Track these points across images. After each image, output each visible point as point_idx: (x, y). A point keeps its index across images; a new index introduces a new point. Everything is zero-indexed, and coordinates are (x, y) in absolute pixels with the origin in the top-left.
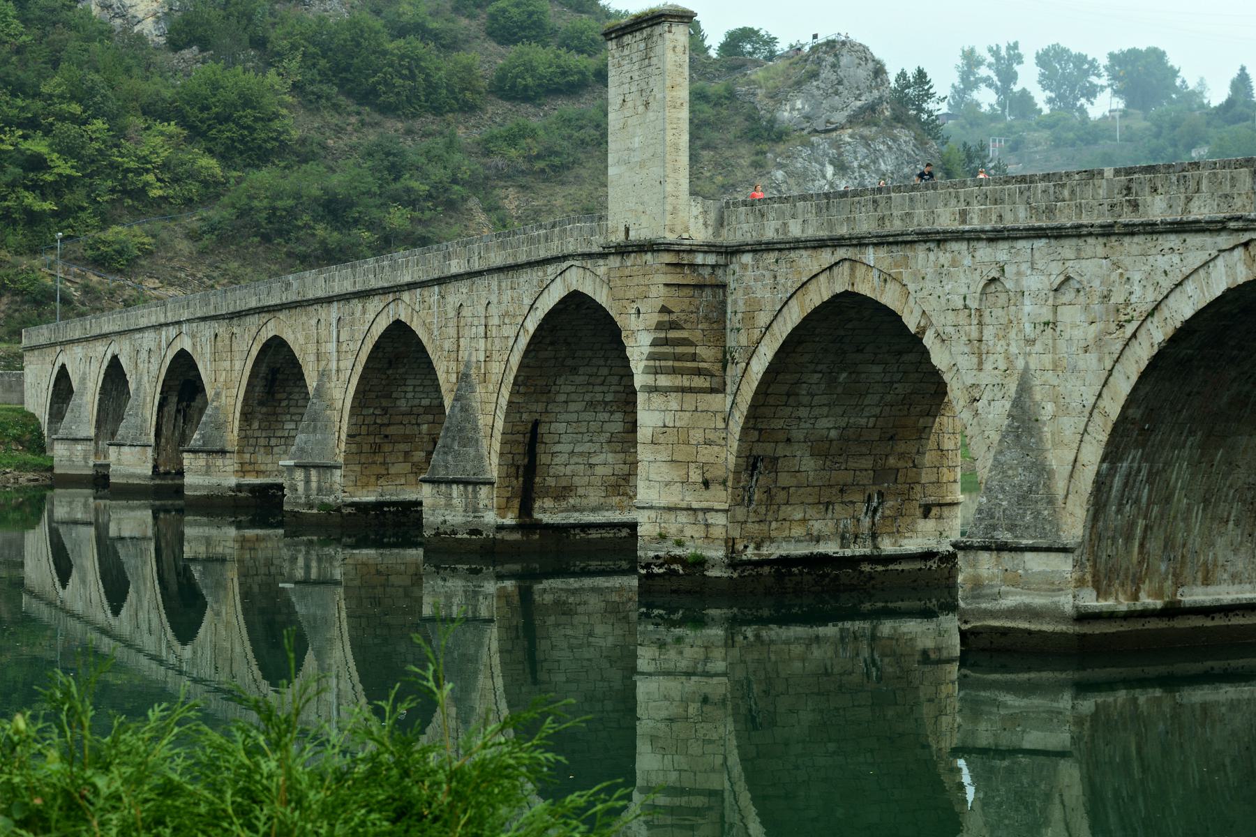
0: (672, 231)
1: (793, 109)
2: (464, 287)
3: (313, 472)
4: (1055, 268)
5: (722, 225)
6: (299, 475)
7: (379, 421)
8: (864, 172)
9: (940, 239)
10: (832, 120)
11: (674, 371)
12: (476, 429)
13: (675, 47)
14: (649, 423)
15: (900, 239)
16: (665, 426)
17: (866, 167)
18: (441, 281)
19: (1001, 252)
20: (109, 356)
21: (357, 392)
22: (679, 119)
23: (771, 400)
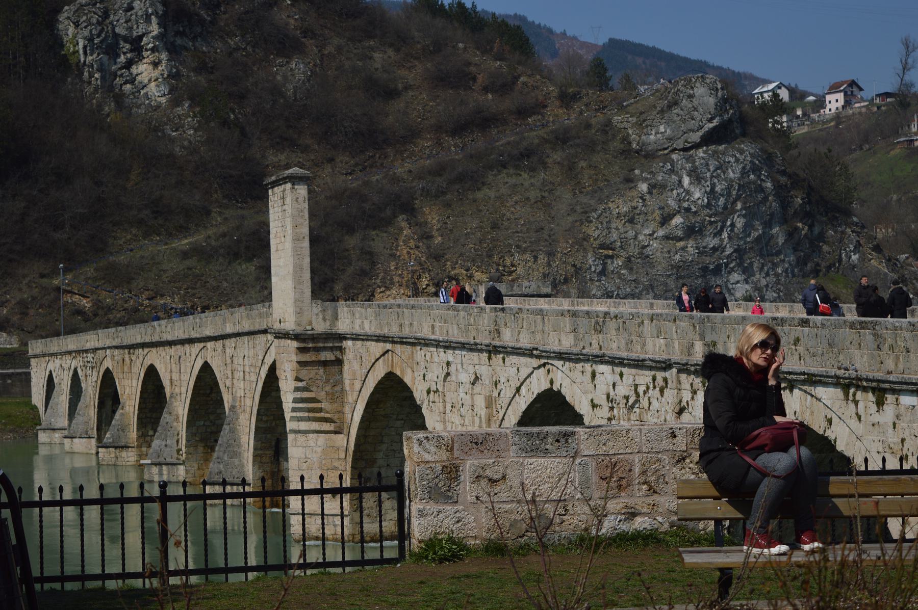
1: (657, 133)
3: (164, 467)
4: (471, 369)
6: (155, 470)
8: (716, 181)
10: (689, 140)
11: (309, 419)
12: (239, 446)
13: (297, 198)
14: (296, 456)
15: (404, 340)
16: (306, 458)
19: (450, 355)
20: (73, 368)
22: (302, 248)
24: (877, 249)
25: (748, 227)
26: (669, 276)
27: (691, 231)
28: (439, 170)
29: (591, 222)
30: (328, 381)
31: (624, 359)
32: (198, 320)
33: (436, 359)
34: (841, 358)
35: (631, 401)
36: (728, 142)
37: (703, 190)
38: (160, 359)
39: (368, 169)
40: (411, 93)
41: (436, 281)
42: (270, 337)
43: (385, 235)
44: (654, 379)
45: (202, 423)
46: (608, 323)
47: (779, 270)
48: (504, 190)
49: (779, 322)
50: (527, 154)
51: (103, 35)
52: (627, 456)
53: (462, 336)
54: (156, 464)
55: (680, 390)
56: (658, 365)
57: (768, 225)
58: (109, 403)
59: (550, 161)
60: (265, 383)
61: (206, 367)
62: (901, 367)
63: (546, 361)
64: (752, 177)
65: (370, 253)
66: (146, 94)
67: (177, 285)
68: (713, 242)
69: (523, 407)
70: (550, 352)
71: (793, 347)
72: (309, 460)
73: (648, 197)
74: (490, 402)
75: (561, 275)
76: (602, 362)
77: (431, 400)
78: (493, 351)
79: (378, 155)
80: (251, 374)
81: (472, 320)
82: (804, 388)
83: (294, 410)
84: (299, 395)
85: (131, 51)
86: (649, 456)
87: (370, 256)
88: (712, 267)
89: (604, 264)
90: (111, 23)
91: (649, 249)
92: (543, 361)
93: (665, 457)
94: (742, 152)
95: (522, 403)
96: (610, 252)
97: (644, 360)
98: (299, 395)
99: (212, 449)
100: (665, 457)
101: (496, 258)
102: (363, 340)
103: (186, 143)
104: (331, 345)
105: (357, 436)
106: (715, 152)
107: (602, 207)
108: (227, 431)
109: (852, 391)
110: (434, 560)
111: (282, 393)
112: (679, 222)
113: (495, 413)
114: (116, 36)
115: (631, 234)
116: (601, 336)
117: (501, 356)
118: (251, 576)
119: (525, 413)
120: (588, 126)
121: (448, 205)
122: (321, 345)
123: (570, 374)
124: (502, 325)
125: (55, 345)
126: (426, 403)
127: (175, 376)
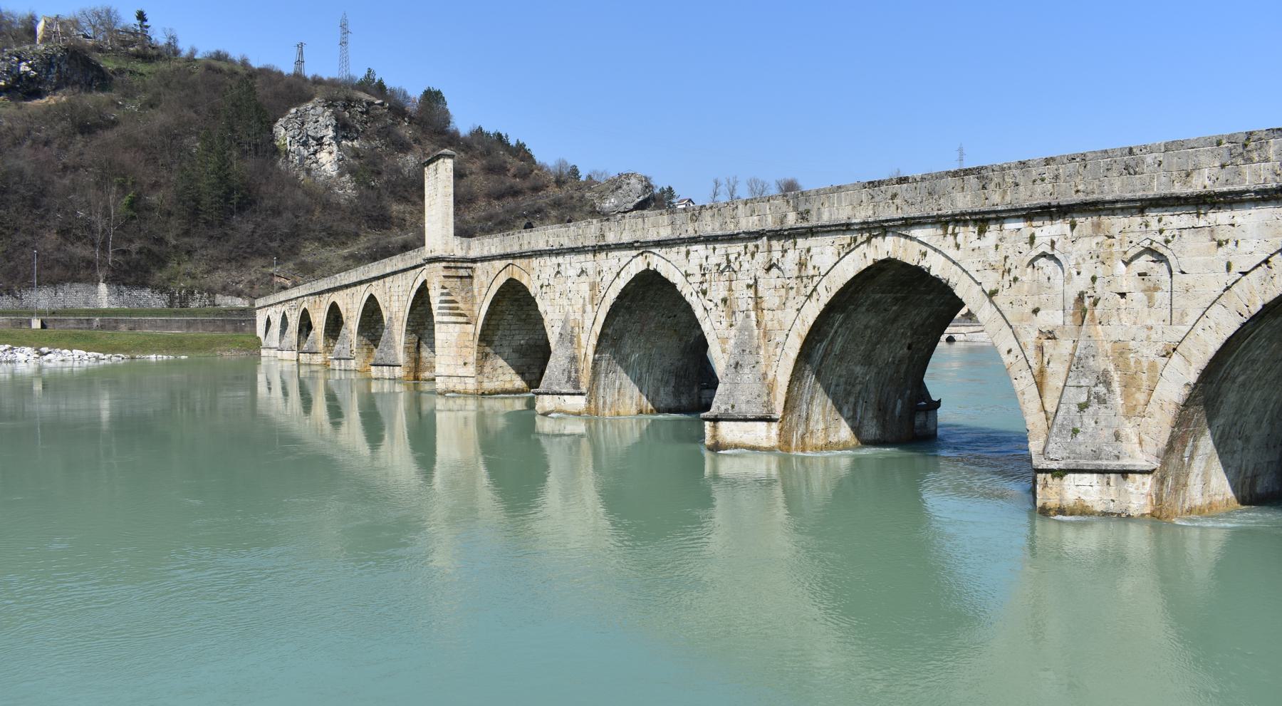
0: (445, 252)
1: (610, 203)
2: (390, 278)
4: (578, 266)
5: (470, 249)
6: (336, 362)
11: (450, 314)
12: (394, 342)
18: (384, 276)
19: (560, 259)
20: (282, 311)
21: (359, 326)
23: (491, 327)
28: (489, 218)
30: (463, 290)
31: (719, 236)
32: (366, 268)
33: (549, 263)
34: (942, 201)
38: (340, 298)
40: (473, 176)
44: (746, 247)
49: (876, 184)
50: (539, 211)
51: (301, 135)
53: (572, 244)
54: (337, 359)
55: (770, 252)
58: (305, 329)
60: (413, 300)
61: (372, 298)
62: (1008, 199)
66: (325, 169)
69: (623, 285)
70: (649, 242)
71: (891, 201)
74: (593, 286)
76: (696, 242)
77: (544, 292)
84: (444, 298)
85: (317, 145)
90: (306, 129)
92: (641, 251)
95: (621, 283)
97: (738, 234)
98: (444, 298)
102: (489, 260)
103: (347, 197)
105: (483, 325)
109: (950, 228)
113: (598, 293)
114: (308, 135)
116: (696, 224)
120: (572, 198)
125: (271, 299)
127: (349, 306)
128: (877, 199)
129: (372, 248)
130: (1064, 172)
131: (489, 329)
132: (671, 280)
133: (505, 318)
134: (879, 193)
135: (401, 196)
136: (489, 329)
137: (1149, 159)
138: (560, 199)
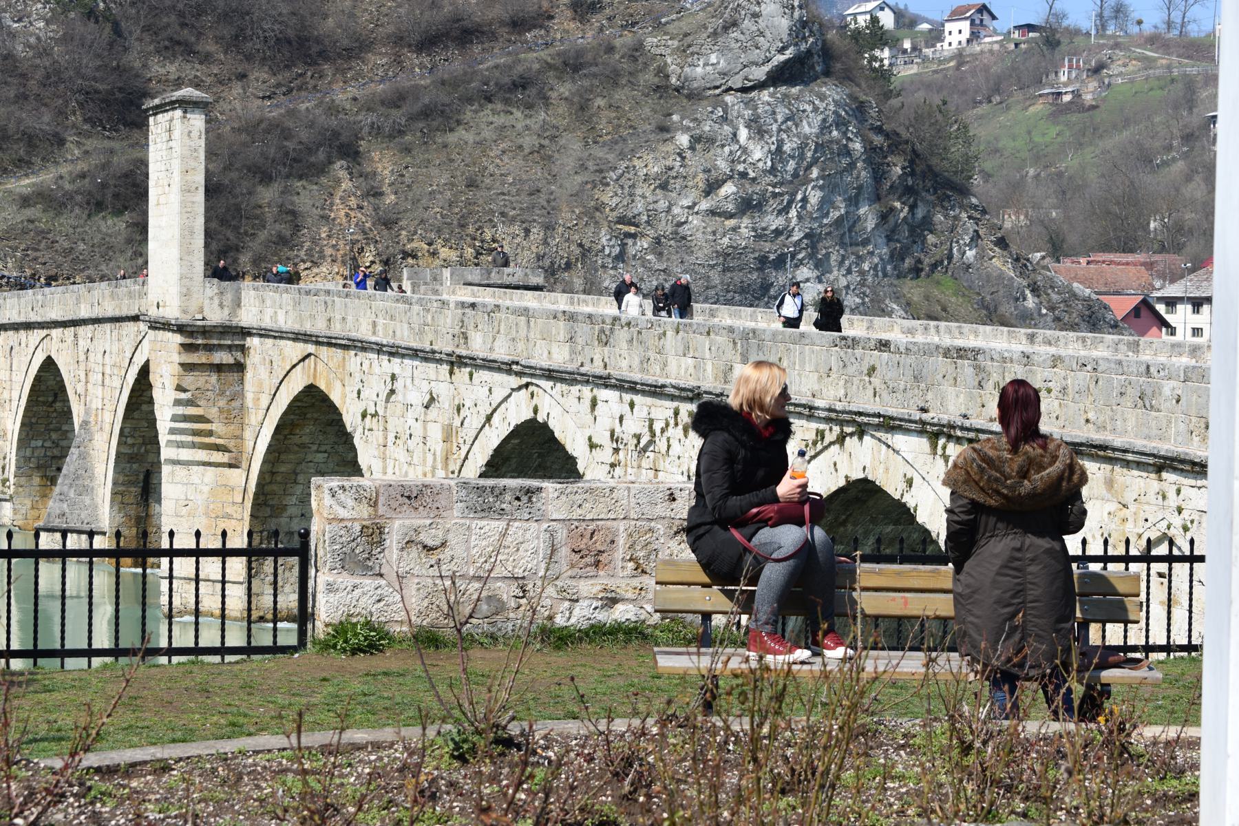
1: (706, 64)
4: (425, 387)
5: (239, 306)
7: (48, 454)
8: (784, 136)
9: (363, 346)
10: (751, 77)
11: (194, 445)
12: (92, 478)
17: (788, 130)
19: (396, 365)
21: (23, 424)
22: (193, 203)
23: (279, 478)
24: (1002, 243)
25: (826, 204)
26: (713, 267)
27: (747, 206)
28: (397, 100)
29: (608, 184)
30: (222, 393)
32: (40, 297)
33: (376, 369)
34: (930, 396)
35: (643, 442)
36: (806, 84)
37: (766, 148)
39: (295, 92)
41: (384, 257)
42: (143, 326)
43: (315, 187)
44: (676, 413)
45: (40, 443)
46: (617, 332)
47: (866, 266)
48: (487, 133)
49: (850, 342)
50: (522, 84)
52: (609, 523)
56: (684, 394)
57: (853, 202)
59: (554, 95)
60: (133, 391)
61: (49, 364)
63: (529, 380)
64: (835, 133)
65: (293, 213)
67: (11, 243)
68: (776, 222)
69: (496, 443)
70: (535, 369)
71: (867, 378)
72: (190, 503)
73: (688, 154)
74: (448, 434)
75: (562, 258)
76: (606, 386)
78: (456, 362)
79: (309, 74)
80: (114, 378)
81: (429, 317)
82: (878, 434)
83: (172, 431)
84: (180, 410)
86: (639, 523)
87: (293, 216)
88: (772, 257)
89: (623, 245)
91: (686, 227)
92: (525, 380)
93: (660, 527)
94: (822, 98)
96: (632, 229)
97: (663, 386)
98: (180, 410)
99: (53, 481)
100: (660, 527)
101: (471, 229)
102: (275, 337)
103: (32, 40)
104: (229, 342)
105: (262, 474)
106: (785, 96)
107: (624, 165)
108: (75, 457)
109: (942, 441)
110: (344, 651)
111: (156, 406)
112: (730, 192)
115: (663, 205)
116: (606, 349)
117: (468, 369)
118: (97, 661)
119: (498, 451)
120: (610, 49)
121: (407, 150)
122: (215, 342)
123: (562, 400)
124: (471, 327)
126: (360, 430)
128: (851, 370)
129: (94, 178)
130: (1073, 385)
131: (276, 482)
132: (570, 449)
133: (309, 457)
134: (853, 360)
135: (171, 39)
136: (276, 482)
137: (1168, 388)
138: (580, 53)
